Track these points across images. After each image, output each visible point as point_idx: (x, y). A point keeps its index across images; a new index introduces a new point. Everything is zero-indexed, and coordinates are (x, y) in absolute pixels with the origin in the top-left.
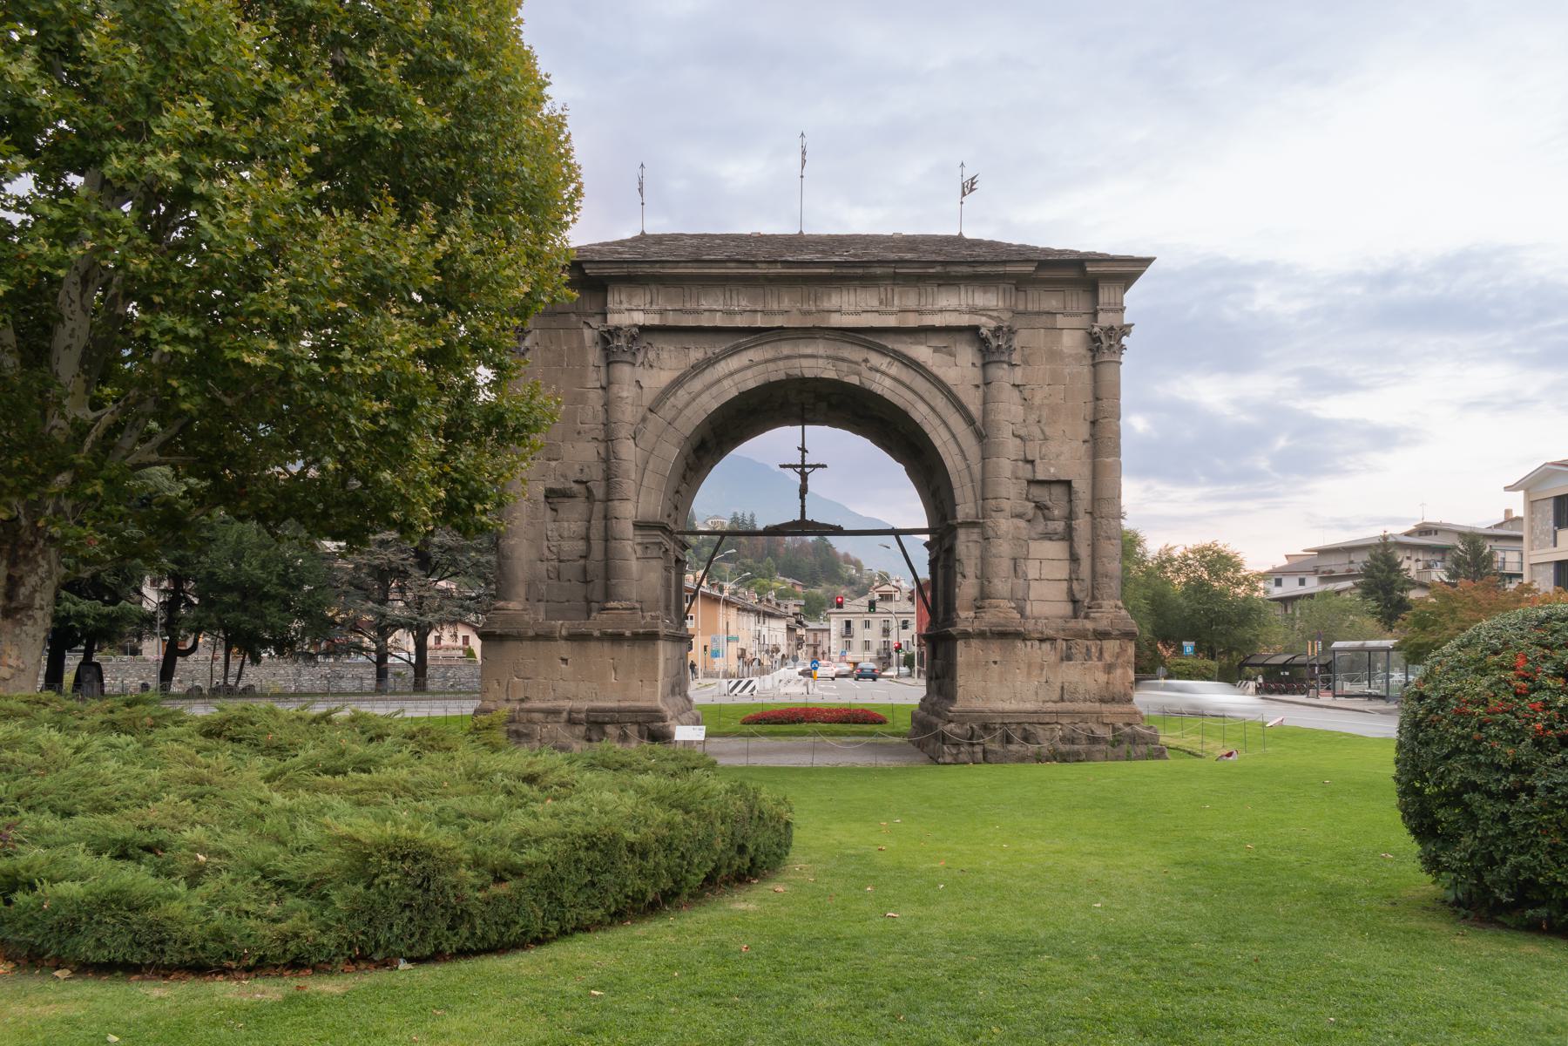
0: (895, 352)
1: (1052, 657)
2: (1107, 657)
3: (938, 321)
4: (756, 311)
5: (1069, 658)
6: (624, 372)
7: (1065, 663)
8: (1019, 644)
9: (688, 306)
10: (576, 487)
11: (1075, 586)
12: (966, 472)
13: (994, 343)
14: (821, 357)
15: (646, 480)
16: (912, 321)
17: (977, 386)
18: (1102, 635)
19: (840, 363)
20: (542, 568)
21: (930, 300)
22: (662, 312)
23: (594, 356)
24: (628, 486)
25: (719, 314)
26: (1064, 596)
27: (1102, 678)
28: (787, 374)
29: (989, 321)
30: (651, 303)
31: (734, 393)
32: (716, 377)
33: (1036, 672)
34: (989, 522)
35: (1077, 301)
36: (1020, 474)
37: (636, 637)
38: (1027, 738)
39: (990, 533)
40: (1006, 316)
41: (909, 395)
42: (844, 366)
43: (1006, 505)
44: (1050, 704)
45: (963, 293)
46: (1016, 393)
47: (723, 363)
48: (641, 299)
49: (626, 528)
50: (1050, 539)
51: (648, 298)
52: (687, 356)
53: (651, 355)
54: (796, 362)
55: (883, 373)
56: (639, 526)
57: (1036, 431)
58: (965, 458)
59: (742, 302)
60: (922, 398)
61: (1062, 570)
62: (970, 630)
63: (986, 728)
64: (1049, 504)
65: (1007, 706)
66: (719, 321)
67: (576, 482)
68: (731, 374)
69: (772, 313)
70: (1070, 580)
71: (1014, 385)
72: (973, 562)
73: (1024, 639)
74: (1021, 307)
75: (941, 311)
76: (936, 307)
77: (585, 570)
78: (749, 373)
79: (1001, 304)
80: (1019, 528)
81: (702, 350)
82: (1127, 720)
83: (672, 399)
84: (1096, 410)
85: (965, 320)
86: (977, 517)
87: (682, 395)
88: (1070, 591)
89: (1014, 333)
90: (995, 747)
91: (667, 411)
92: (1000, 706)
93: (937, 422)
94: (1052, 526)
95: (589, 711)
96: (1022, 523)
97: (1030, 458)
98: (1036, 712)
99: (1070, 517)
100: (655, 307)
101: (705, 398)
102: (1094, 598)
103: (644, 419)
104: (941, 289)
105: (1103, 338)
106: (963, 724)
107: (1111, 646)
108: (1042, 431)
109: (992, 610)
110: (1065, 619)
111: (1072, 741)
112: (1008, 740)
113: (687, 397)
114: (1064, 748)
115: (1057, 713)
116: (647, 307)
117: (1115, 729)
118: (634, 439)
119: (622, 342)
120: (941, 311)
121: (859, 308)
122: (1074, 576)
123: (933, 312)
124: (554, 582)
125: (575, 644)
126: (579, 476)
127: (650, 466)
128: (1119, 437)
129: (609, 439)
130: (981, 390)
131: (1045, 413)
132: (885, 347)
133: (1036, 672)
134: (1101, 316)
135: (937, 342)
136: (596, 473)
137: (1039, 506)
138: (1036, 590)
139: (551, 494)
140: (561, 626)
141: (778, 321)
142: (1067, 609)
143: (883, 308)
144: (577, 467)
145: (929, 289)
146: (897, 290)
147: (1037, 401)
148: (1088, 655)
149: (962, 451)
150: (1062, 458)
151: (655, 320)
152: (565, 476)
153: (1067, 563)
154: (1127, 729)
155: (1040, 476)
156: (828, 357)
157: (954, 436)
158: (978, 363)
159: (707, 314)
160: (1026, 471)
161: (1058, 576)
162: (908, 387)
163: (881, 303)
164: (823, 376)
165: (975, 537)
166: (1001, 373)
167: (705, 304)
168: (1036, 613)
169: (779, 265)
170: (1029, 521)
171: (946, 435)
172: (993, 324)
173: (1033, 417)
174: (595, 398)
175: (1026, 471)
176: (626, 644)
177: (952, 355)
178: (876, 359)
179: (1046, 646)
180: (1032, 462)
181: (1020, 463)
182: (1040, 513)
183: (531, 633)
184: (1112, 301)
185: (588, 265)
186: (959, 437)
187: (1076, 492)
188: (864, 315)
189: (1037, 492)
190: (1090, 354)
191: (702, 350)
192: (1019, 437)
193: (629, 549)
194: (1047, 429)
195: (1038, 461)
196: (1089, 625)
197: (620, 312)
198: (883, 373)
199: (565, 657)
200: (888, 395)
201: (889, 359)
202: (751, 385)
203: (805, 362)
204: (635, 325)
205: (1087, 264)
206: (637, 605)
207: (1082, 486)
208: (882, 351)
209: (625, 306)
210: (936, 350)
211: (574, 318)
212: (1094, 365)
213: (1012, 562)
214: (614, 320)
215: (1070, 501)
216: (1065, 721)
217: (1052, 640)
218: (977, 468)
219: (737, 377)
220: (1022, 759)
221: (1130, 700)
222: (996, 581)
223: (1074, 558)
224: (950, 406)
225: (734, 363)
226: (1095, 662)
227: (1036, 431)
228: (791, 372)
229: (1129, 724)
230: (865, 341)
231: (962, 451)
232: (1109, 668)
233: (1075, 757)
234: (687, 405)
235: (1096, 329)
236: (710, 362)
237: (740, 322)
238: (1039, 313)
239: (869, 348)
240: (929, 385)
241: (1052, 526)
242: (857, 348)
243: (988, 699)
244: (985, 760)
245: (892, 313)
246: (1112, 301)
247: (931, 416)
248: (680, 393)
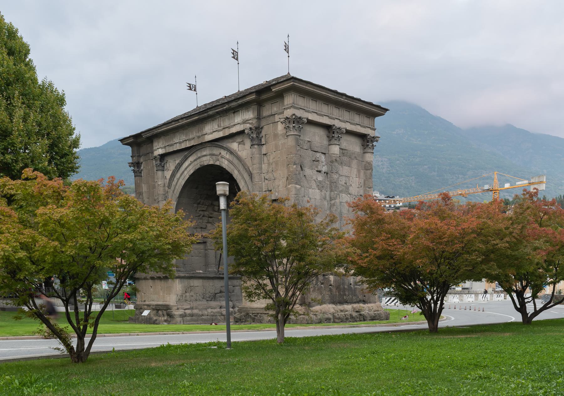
9: (171, 143)
22: (165, 147)
28: (201, 165)
40: (254, 121)
41: (232, 167)
66: (178, 148)
68: (186, 169)
89: (262, 128)
104: (235, 114)
132: (223, 146)
150: (280, 187)
202: (192, 172)
205: (272, 88)
228: (202, 163)
230: (219, 145)
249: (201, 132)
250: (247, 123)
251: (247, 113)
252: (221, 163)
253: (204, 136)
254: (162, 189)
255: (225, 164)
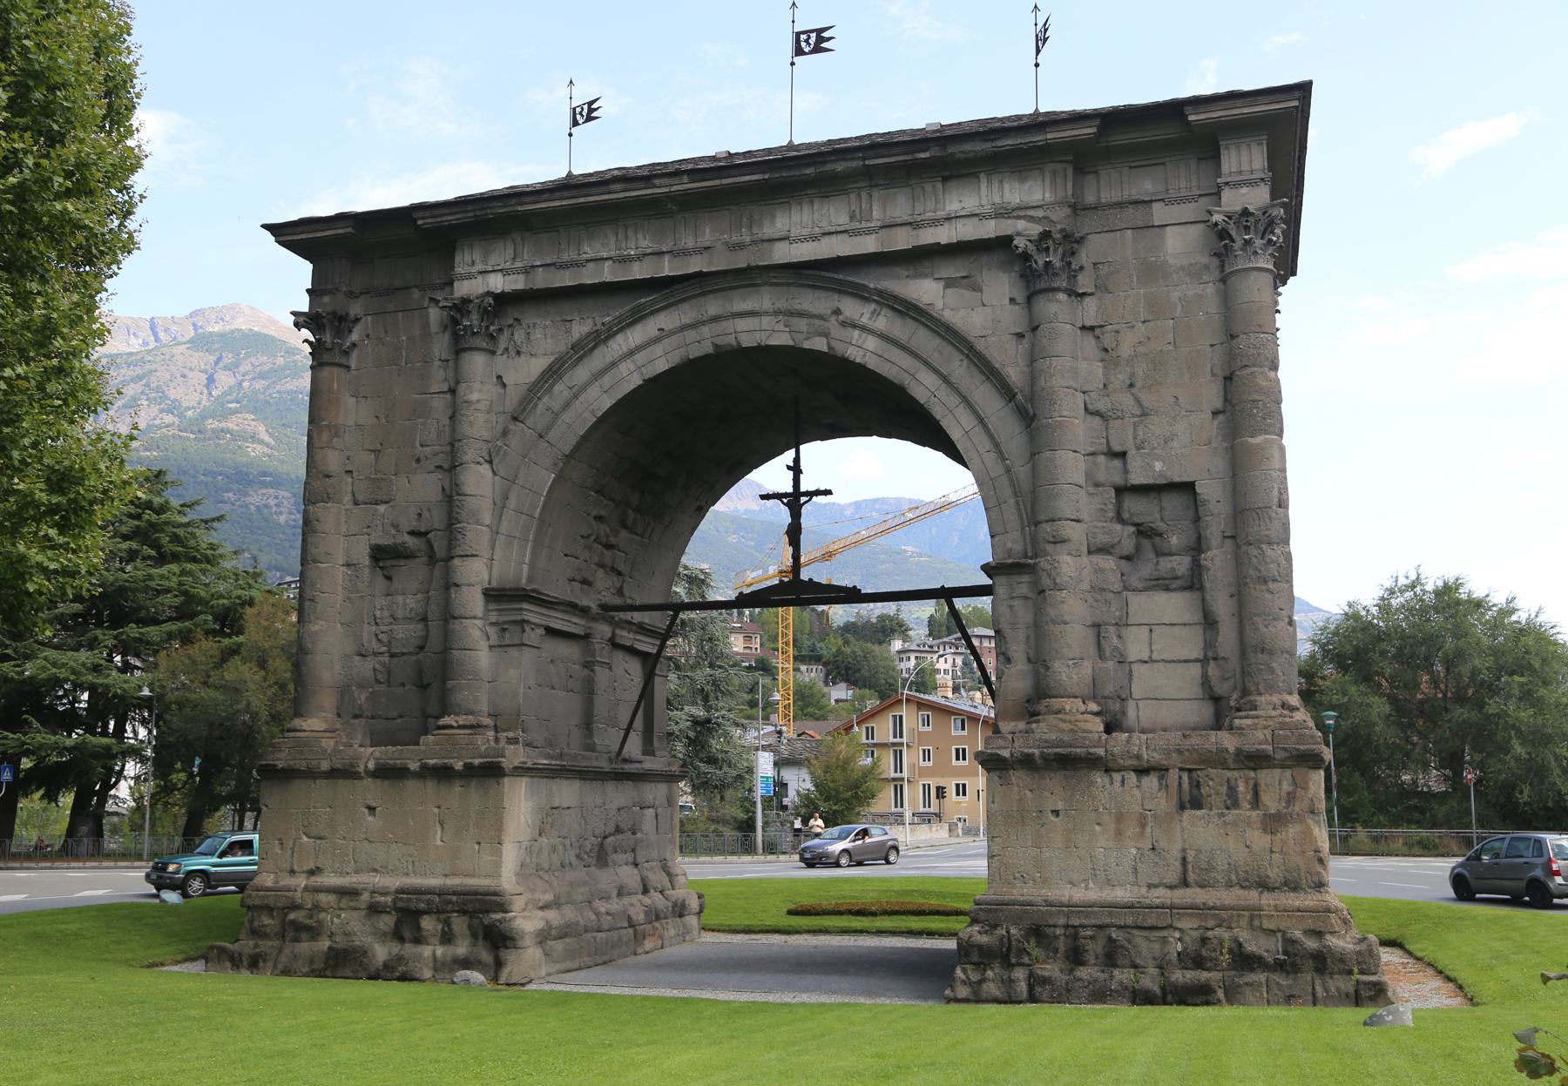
0: (881, 293)
1: (1163, 803)
2: (1271, 802)
3: (944, 235)
4: (661, 253)
5: (1196, 804)
6: (477, 363)
7: (1188, 813)
8: (1099, 778)
9: (565, 257)
10: (411, 542)
11: (1213, 670)
12: (1005, 481)
13: (1041, 260)
14: (766, 313)
15: (504, 528)
16: (902, 240)
17: (1020, 336)
18: (1255, 760)
19: (795, 321)
20: (366, 667)
21: (931, 205)
22: (528, 270)
23: (441, 346)
24: (476, 536)
25: (607, 264)
26: (1196, 691)
27: (1259, 840)
28: (716, 346)
29: (1030, 225)
30: (514, 259)
31: (636, 381)
32: (609, 359)
33: (1131, 830)
34: (1044, 564)
35: (1184, 177)
36: (1101, 476)
37: (470, 772)
38: (1111, 957)
39: (1046, 582)
40: (1060, 215)
41: (906, 361)
42: (802, 324)
43: (1071, 530)
44: (1161, 891)
45: (984, 185)
46: (1089, 342)
47: (620, 338)
48: (502, 254)
49: (472, 601)
50: (1167, 589)
51: (510, 252)
52: (568, 331)
53: (519, 336)
54: (728, 325)
55: (863, 329)
56: (493, 595)
57: (1127, 402)
58: (1002, 457)
59: (643, 242)
60: (926, 363)
61: (1189, 644)
62: (1006, 753)
63: (1037, 932)
64: (1161, 526)
65: (1079, 894)
66: (608, 274)
67: (412, 533)
68: (631, 353)
69: (686, 253)
70: (1204, 661)
71: (1083, 328)
72: (1022, 635)
73: (1108, 771)
74: (1090, 198)
75: (949, 219)
76: (941, 214)
77: (420, 671)
78: (658, 349)
79: (1047, 195)
80: (1101, 570)
81: (590, 322)
82: (1310, 924)
83: (546, 399)
84: (1231, 356)
85: (989, 229)
86: (1026, 556)
87: (561, 390)
88: (1206, 682)
89: (1080, 241)
90: (1052, 969)
91: (538, 418)
92: (1067, 893)
93: (953, 400)
94: (1166, 564)
95: (401, 891)
96: (1108, 563)
97: (1117, 448)
98: (1130, 906)
99: (1197, 548)
100: (518, 264)
101: (593, 392)
102: (1245, 692)
103: (505, 434)
104: (949, 184)
105: (1233, 233)
106: (994, 927)
107: (1275, 783)
108: (1138, 400)
109: (1051, 719)
110: (1187, 730)
111: (1199, 963)
112: (1076, 957)
113: (567, 394)
114: (1180, 976)
115: (1172, 907)
116: (508, 265)
117: (1289, 942)
118: (490, 462)
119: (473, 320)
120: (949, 219)
121: (817, 230)
122: (1210, 654)
123: (935, 222)
124: (383, 688)
125: (387, 783)
126: (414, 525)
127: (512, 502)
128: (1279, 402)
129: (452, 467)
130: (1026, 343)
131: (1141, 368)
133: (1131, 830)
134: (1227, 195)
135: (950, 270)
136: (437, 519)
137: (1144, 532)
138: (1144, 680)
139: (381, 555)
140: (370, 756)
141: (695, 265)
142: (1201, 712)
143: (856, 225)
144: (413, 510)
145: (928, 187)
146: (876, 194)
147: (1125, 350)
148: (1233, 801)
149: (997, 445)
150: (1175, 444)
151: (517, 283)
152: (396, 526)
153: (1200, 629)
154: (1311, 944)
155: (1137, 479)
156: (776, 313)
157: (981, 421)
158: (1021, 297)
159: (591, 265)
160: (1110, 472)
161: (1184, 655)
162: (904, 348)
163: (852, 218)
164: (773, 342)
165: (1024, 589)
166: (1056, 308)
167: (589, 251)
168: (1145, 723)
169: (685, 178)
170: (1128, 558)
171: (968, 421)
172: (1035, 230)
173: (1119, 379)
174: (439, 404)
175: (1110, 472)
176: (457, 782)
177: (977, 288)
178: (852, 309)
179: (1151, 782)
180: (1122, 455)
181: (1102, 459)
182: (1146, 543)
183: (325, 766)
184: (1245, 167)
185: (420, 214)
186: (992, 423)
187: (1204, 502)
188: (825, 240)
189: (1133, 505)
190: (1215, 262)
191: (590, 322)
192: (1097, 413)
193: (477, 633)
194: (1142, 396)
195: (1132, 452)
196: (1228, 741)
197: (470, 277)
198: (863, 329)
199: (374, 805)
200: (872, 363)
201: (873, 306)
202: (662, 366)
203: (742, 324)
204: (489, 294)
206: (488, 721)
207: (1211, 490)
208: (861, 294)
209: (479, 267)
210: (950, 283)
211: (416, 294)
212: (1224, 280)
213: (1091, 633)
214: (463, 289)
215: (1197, 519)
216: (1184, 924)
217: (1162, 770)
218: (1022, 472)
219: (640, 357)
220: (1100, 995)
221: (1320, 885)
222: (1057, 665)
223: (1209, 622)
224: (975, 371)
225: (636, 336)
226: (1245, 812)
227: (1127, 402)
229: (1319, 934)
231: (997, 445)
232: (1273, 823)
233: (1197, 995)
234: (567, 405)
235: (1217, 218)
236: (599, 339)
237: (639, 272)
238: (1120, 205)
239: (840, 292)
240: (938, 341)
241: (1166, 564)
242: (823, 294)
243: (1045, 881)
244: (1033, 999)
245: (869, 232)
246: (1245, 167)
247: (944, 393)
248: (558, 388)
249: (750, 228)
250: (1019, 217)
251: (1016, 184)
252: (834, 344)
253: (766, 245)
254: (481, 418)
255: (863, 350)
